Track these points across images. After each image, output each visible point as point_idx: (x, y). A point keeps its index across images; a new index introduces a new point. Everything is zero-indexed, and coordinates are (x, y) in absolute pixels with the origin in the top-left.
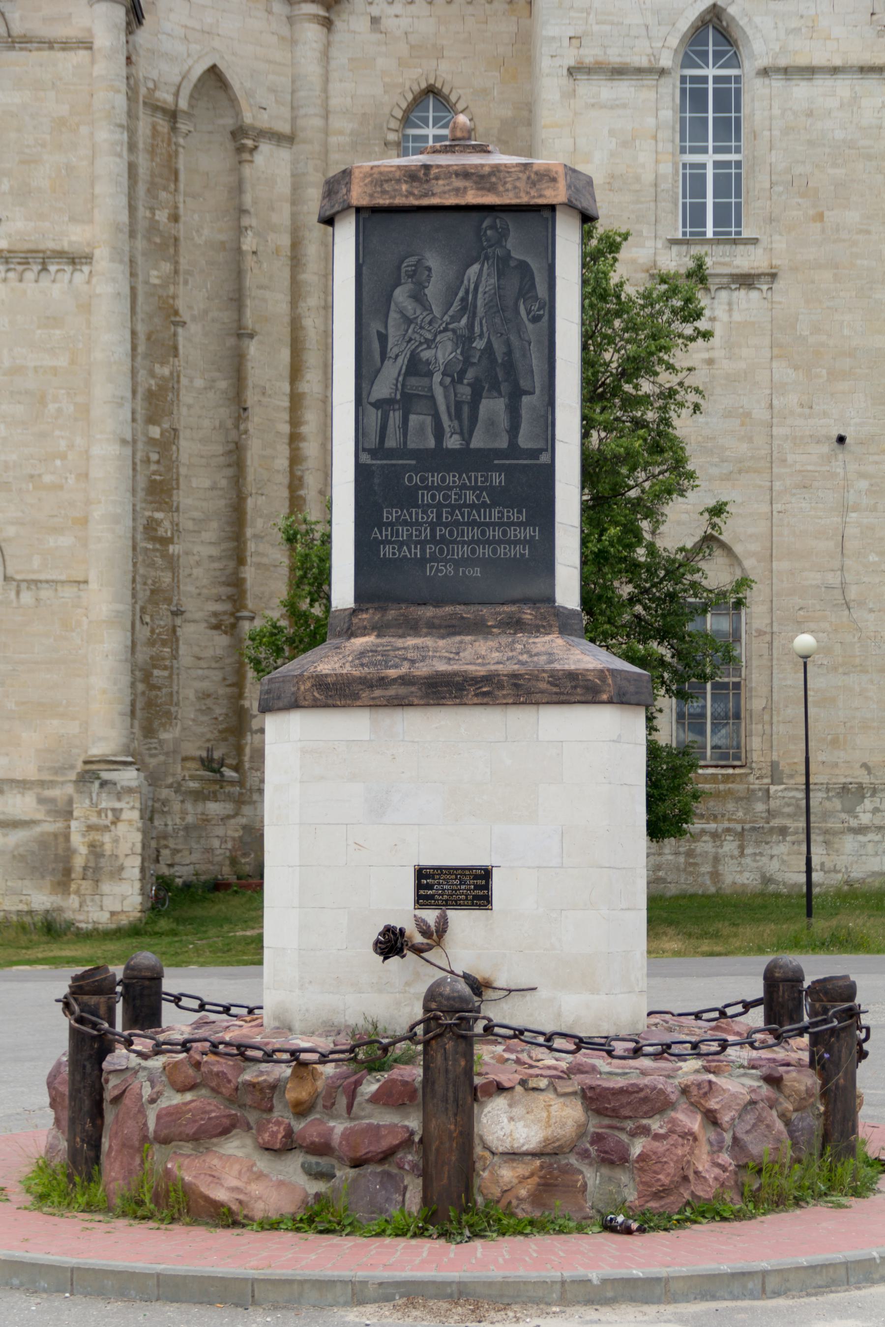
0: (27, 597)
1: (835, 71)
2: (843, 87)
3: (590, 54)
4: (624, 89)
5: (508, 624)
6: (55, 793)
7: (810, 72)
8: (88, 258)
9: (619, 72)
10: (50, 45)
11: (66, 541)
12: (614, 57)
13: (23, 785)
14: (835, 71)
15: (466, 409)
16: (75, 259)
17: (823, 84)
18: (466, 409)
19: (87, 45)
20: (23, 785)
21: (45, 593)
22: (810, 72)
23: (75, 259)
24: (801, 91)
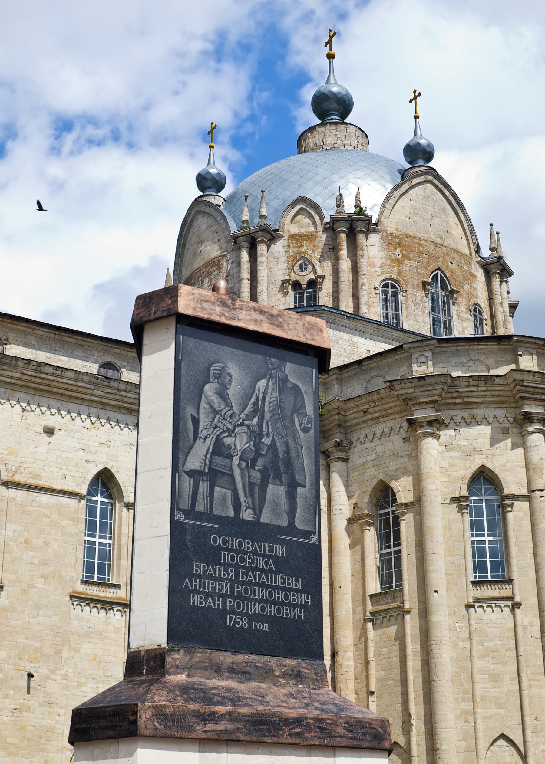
5: (291, 675)
15: (257, 490)
18: (257, 490)
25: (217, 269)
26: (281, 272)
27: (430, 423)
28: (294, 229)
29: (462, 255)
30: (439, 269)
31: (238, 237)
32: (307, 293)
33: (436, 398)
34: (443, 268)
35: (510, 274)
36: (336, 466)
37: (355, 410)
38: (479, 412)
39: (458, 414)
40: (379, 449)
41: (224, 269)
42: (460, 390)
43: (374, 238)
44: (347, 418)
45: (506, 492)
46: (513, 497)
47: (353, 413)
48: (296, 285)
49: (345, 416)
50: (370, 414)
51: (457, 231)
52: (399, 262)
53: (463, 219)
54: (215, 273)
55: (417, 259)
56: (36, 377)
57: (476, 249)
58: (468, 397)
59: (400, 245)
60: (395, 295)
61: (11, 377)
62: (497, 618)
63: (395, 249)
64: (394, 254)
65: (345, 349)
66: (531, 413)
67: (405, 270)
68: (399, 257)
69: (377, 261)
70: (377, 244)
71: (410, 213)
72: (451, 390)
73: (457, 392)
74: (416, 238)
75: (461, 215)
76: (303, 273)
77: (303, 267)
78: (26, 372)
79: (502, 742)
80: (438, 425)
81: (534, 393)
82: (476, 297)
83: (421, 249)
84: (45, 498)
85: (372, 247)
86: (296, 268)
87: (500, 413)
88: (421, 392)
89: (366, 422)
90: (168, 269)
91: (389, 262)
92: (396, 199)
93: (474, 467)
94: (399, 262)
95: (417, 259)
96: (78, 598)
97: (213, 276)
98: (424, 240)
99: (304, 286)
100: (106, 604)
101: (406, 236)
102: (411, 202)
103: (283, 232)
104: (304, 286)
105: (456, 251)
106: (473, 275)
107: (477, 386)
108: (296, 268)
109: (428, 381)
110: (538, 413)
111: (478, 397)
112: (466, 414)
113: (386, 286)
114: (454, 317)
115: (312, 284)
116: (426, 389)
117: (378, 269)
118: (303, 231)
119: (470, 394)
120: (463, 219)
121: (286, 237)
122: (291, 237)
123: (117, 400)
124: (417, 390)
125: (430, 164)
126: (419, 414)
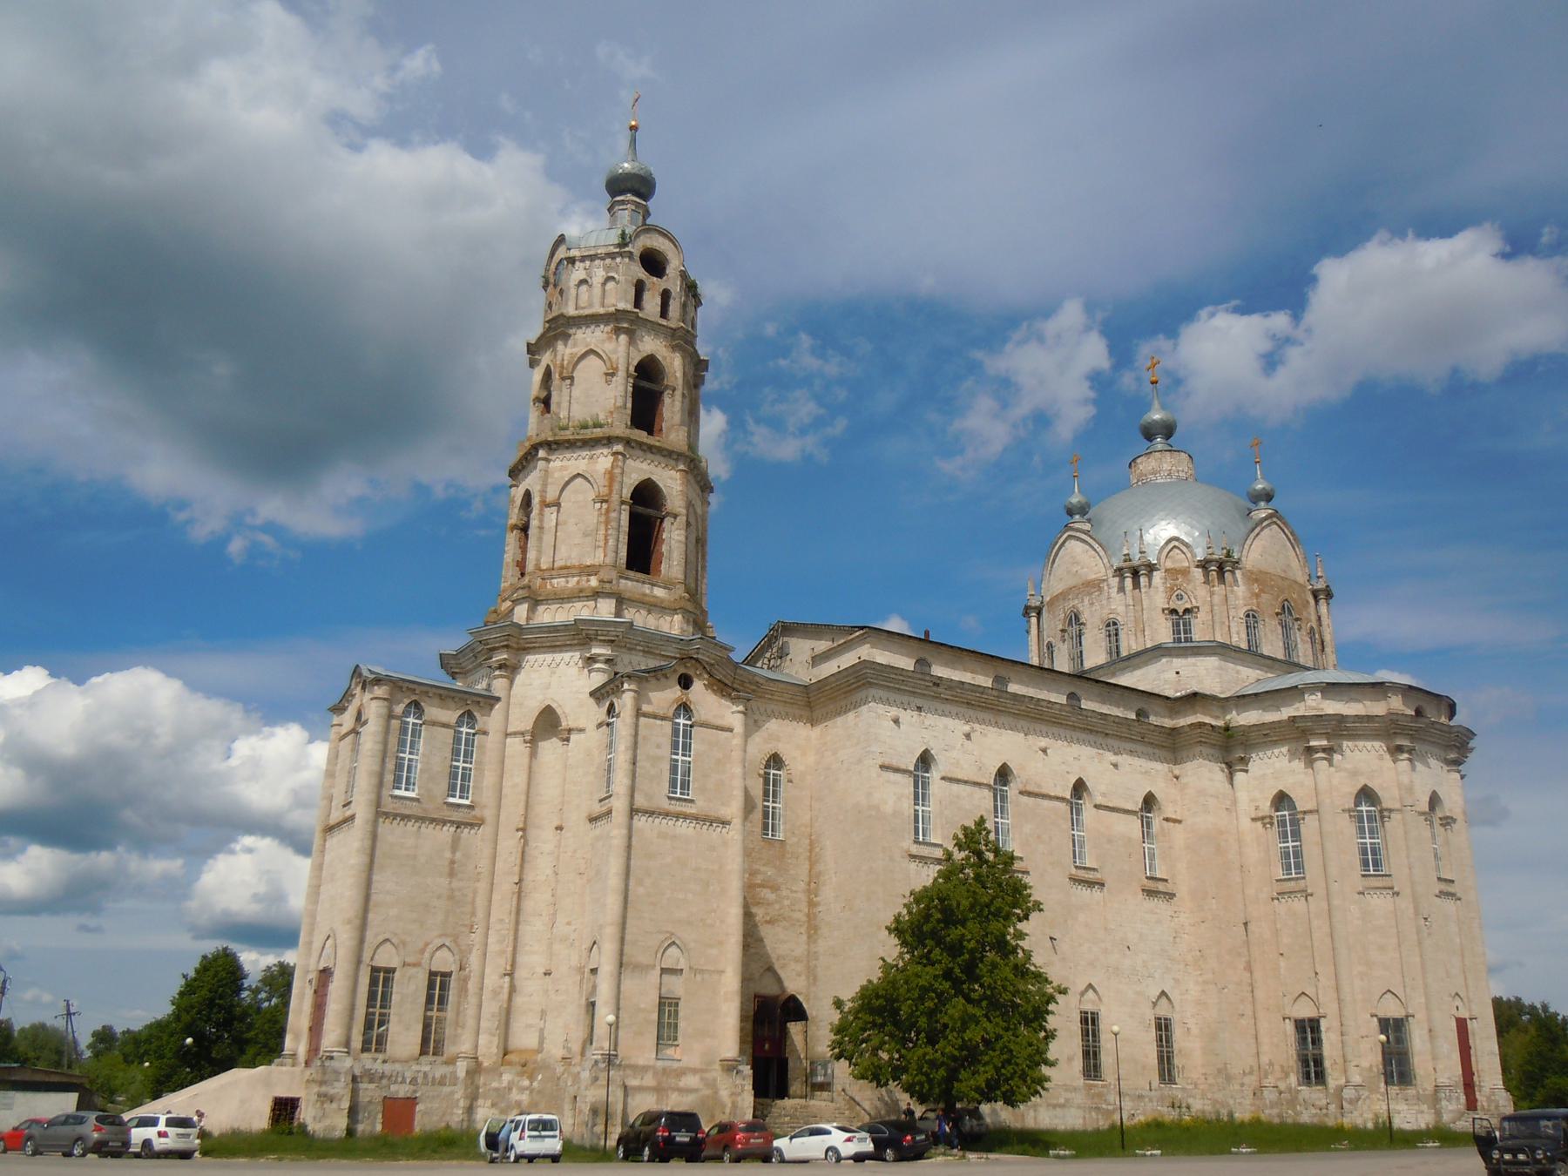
0: (699, 977)
1: (966, 782)
2: (968, 788)
3: (887, 761)
4: (898, 777)
6: (707, 1075)
7: (958, 781)
8: (728, 823)
9: (897, 770)
10: (718, 728)
11: (714, 952)
12: (895, 763)
13: (695, 1071)
14: (966, 782)
16: (725, 823)
17: (962, 787)
19: (731, 730)
20: (695, 1071)
21: (706, 976)
22: (958, 781)
23: (725, 823)
24: (955, 787)
27: (1324, 750)
28: (1169, 564)
36: (1239, 776)
40: (1277, 765)
45: (1384, 805)
46: (1390, 811)
48: (1173, 611)
52: (1257, 596)
59: (1256, 580)
62: (1380, 903)
77: (1180, 597)
79: (1389, 995)
84: (1046, 803)
87: (1377, 744)
93: (1359, 786)
96: (1076, 880)
100: (1090, 884)
115: (1187, 611)
118: (1177, 565)
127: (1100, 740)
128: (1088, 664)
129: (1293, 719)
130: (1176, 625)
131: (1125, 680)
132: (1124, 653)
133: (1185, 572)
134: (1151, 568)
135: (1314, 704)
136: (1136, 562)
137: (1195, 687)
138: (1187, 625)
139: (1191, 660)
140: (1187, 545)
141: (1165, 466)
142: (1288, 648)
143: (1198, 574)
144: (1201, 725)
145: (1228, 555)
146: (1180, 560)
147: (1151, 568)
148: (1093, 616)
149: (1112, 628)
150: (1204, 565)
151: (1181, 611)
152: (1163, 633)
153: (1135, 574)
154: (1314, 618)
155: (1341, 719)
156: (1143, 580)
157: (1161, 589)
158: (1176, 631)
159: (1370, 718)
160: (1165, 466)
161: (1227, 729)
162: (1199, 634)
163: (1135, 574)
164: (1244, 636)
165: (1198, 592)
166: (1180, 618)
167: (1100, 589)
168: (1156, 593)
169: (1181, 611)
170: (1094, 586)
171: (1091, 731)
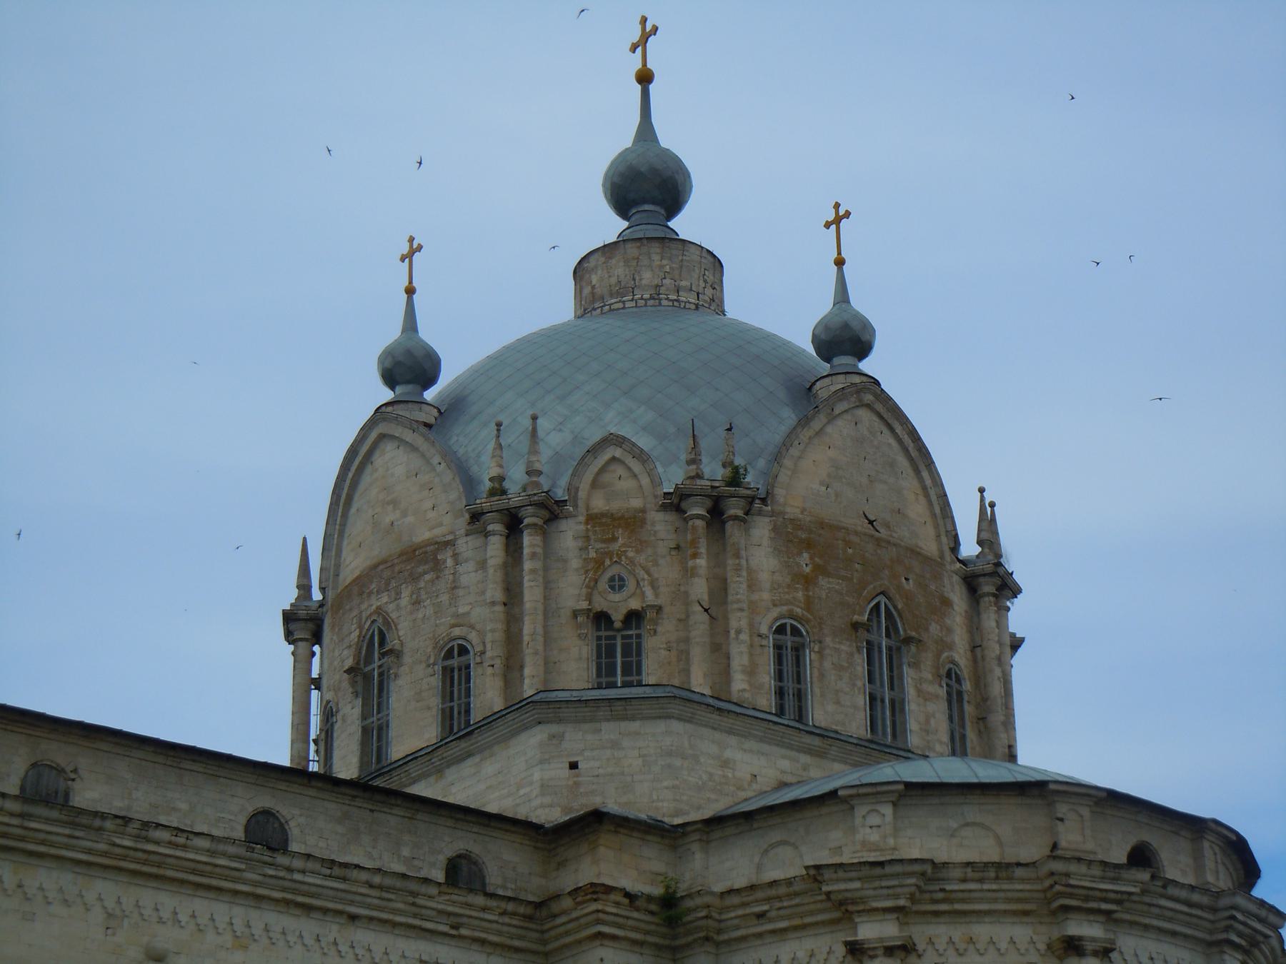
25: (432, 570)
26: (571, 591)
28: (599, 503)
29: (927, 560)
30: (882, 593)
31: (483, 514)
32: (624, 637)
33: (902, 902)
34: (892, 592)
35: (1015, 591)
37: (740, 912)
38: (983, 931)
39: (941, 932)
41: (447, 572)
42: (948, 887)
43: (761, 530)
44: (723, 925)
47: (736, 917)
48: (601, 619)
49: (720, 921)
50: (771, 921)
51: (917, 510)
52: (808, 581)
53: (928, 482)
54: (427, 577)
55: (843, 573)
56: (136, 850)
57: (952, 545)
58: (963, 901)
59: (808, 545)
60: (798, 650)
61: (89, 851)
63: (800, 554)
64: (798, 565)
65: (711, 775)
66: (1080, 938)
67: (820, 598)
68: (808, 570)
69: (764, 577)
70: (766, 542)
71: (829, 475)
72: (931, 888)
73: (943, 890)
74: (839, 528)
75: (925, 474)
76: (616, 597)
77: (617, 584)
78: (118, 841)
80: (903, 954)
81: (1087, 899)
82: (950, 647)
83: (850, 551)
85: (759, 550)
86: (603, 584)
87: (1021, 932)
88: (875, 889)
89: (760, 935)
90: (305, 539)
91: (788, 580)
92: (802, 447)
94: (808, 581)
95: (843, 573)
97: (422, 584)
98: (856, 533)
99: (618, 625)
101: (822, 524)
102: (831, 453)
103: (576, 506)
104: (618, 625)
105: (915, 552)
106: (947, 603)
107: (981, 881)
108: (603, 584)
109: (888, 870)
110: (1094, 940)
111: (981, 900)
112: (957, 932)
113: (781, 630)
114: (911, 692)
115: (634, 618)
116: (884, 883)
117: (766, 596)
118: (616, 506)
119: (966, 895)
120: (928, 482)
121: (582, 519)
122: (592, 518)
123: (284, 890)
124: (866, 886)
125: (866, 366)
126: (868, 931)
127: (332, 930)
128: (397, 751)
129: (816, 872)
130: (604, 656)
131: (465, 785)
132: (476, 716)
133: (632, 522)
134: (552, 510)
135: (872, 834)
136: (515, 495)
137: (596, 802)
138: (634, 653)
139: (610, 730)
140: (642, 456)
141: (647, 277)
142: (886, 712)
143: (661, 525)
144: (598, 890)
145: (735, 479)
146: (627, 492)
147: (552, 510)
148: (417, 630)
149: (455, 665)
150: (675, 503)
151: (618, 617)
152: (575, 668)
153: (513, 524)
154: (960, 639)
155: (933, 870)
156: (529, 541)
157: (575, 563)
158: (605, 669)
159: (1003, 869)
160: (647, 277)
161: (669, 901)
162: (652, 671)
163: (513, 524)
164: (767, 678)
165: (661, 574)
166: (617, 638)
167: (437, 566)
168: (563, 573)
169: (618, 617)
170: (420, 560)
171: (308, 909)
